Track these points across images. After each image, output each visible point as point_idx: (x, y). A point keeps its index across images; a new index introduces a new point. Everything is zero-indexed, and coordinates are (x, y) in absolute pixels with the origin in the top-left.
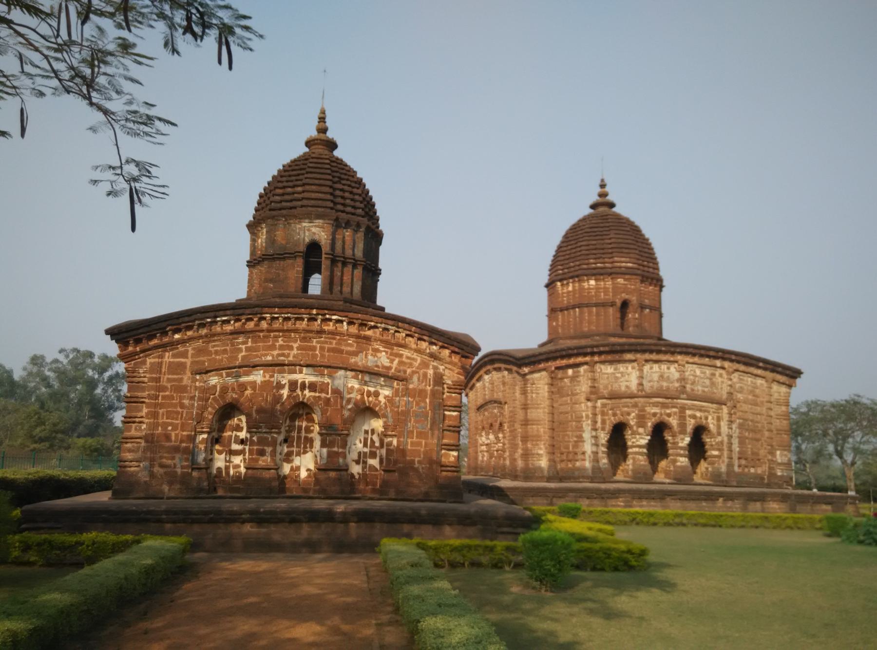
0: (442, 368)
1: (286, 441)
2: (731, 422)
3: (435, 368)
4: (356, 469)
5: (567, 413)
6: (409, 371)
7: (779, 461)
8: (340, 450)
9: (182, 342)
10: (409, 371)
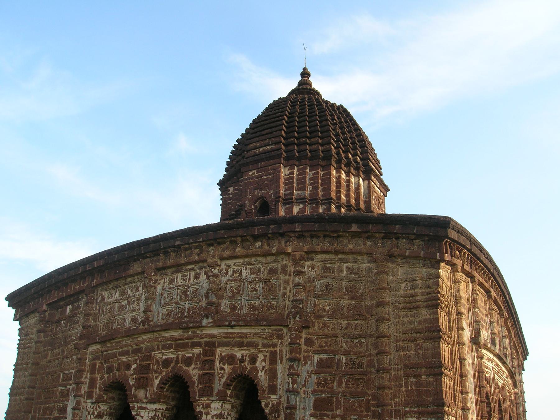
5: (54, 373)
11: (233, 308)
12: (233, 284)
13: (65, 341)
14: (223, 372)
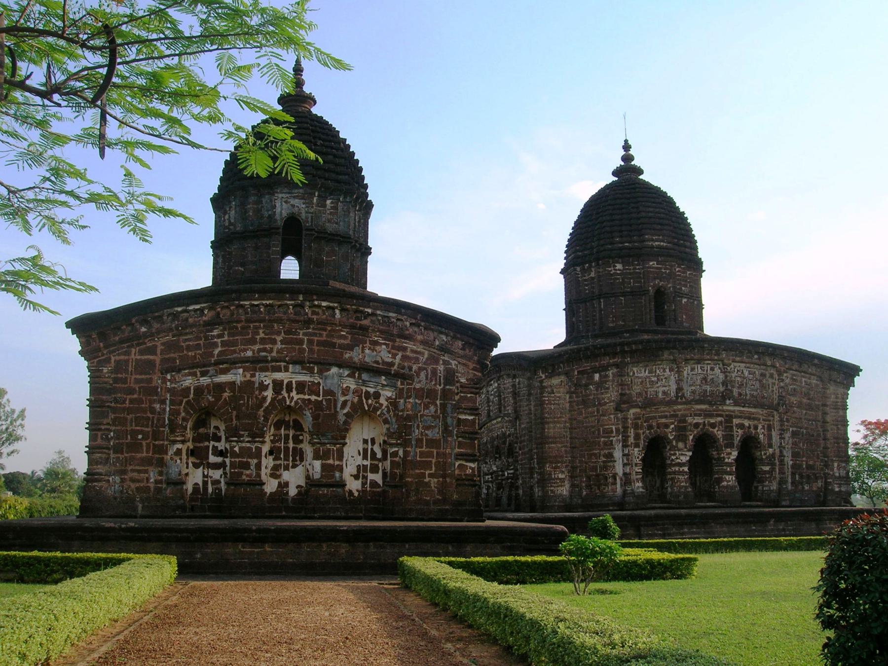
0: (453, 362)
1: (271, 452)
2: (782, 431)
3: (445, 363)
4: (354, 486)
5: (593, 427)
6: (415, 367)
7: (837, 475)
8: (337, 463)
9: (151, 335)
10: (415, 367)
11: (740, 394)
12: (739, 379)
13: (599, 404)
14: (738, 434)
